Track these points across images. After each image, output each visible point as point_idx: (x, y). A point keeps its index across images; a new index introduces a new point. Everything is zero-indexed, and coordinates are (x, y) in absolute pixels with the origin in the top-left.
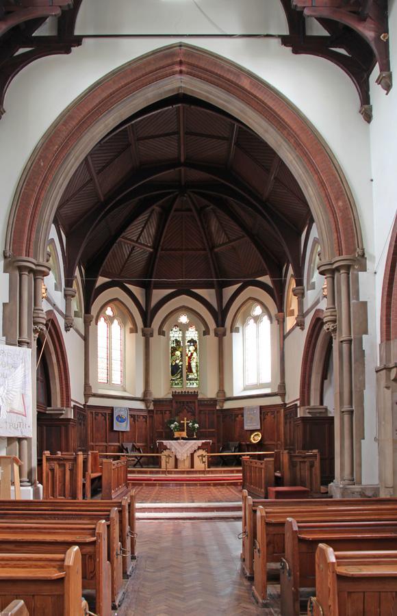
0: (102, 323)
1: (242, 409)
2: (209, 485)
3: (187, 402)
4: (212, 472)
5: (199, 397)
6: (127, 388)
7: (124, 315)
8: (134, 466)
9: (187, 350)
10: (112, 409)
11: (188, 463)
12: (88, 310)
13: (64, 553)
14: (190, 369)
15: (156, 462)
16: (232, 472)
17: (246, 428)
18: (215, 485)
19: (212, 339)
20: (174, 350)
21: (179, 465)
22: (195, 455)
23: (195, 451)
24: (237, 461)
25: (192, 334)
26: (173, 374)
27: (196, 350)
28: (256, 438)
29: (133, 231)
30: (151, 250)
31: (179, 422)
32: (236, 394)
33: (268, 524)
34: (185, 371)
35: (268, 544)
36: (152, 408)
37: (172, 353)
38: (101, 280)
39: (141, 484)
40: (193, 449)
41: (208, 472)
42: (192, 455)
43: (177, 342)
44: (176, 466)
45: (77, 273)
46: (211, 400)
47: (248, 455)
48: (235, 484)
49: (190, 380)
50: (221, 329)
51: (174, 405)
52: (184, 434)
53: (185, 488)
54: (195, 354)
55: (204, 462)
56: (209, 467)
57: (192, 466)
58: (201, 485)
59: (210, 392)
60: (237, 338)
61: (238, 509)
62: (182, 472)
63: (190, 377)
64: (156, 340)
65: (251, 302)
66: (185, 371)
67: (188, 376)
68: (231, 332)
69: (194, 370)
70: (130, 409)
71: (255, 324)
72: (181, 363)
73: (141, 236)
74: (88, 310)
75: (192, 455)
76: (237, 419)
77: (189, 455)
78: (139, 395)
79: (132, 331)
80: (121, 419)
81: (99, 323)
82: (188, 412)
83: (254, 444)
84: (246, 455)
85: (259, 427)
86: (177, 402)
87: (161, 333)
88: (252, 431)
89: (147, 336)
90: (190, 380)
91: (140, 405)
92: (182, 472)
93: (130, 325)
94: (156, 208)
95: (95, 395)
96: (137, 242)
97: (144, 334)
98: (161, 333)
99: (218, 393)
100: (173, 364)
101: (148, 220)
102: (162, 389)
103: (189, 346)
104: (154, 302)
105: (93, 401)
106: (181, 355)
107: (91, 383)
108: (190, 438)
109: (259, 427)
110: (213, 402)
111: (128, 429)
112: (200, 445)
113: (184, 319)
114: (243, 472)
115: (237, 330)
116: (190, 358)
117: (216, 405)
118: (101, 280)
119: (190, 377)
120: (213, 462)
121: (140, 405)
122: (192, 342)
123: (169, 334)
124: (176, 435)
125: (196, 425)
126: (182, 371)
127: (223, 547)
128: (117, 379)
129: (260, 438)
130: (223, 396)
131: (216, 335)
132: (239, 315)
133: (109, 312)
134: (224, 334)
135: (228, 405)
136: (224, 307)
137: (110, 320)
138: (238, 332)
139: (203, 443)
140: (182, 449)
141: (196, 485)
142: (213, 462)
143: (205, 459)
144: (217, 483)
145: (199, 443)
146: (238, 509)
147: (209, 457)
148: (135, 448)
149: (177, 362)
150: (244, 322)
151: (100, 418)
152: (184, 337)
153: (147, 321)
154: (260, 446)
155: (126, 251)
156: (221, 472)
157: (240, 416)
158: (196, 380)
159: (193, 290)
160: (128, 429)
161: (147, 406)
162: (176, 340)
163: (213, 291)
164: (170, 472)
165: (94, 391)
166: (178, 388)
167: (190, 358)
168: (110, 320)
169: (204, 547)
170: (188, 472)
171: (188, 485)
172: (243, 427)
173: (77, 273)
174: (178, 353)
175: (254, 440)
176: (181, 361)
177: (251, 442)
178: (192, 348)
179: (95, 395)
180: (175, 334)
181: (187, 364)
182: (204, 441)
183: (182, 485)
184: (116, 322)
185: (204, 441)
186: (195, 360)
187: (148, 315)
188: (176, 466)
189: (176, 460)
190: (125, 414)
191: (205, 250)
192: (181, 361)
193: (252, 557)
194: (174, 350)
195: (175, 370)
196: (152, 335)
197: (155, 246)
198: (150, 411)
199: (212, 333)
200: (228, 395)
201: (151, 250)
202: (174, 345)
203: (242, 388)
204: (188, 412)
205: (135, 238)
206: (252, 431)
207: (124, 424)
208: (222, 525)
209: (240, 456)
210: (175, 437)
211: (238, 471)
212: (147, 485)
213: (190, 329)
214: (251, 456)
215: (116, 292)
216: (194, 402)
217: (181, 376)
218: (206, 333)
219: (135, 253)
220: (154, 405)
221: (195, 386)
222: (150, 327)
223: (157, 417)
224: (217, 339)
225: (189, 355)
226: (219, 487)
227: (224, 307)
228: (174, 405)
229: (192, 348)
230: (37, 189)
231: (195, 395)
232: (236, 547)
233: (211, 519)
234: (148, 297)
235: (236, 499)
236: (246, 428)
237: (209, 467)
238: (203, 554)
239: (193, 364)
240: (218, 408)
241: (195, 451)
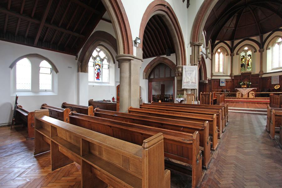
0: (217, 55)
1: (271, 77)
2: (255, 103)
3: (247, 76)
4: (257, 99)
5: (252, 74)
6: (225, 73)
7: (224, 50)
8: (227, 96)
9: (247, 58)
10: (220, 79)
11: (246, 96)
12: (212, 51)
13: (204, 123)
14: (248, 65)
15: (235, 95)
16: (265, 99)
17: (272, 83)
18: (257, 103)
19: (258, 54)
21: (243, 96)
22: (250, 93)
23: (250, 92)
24: (268, 95)
25: (249, 53)
26: (241, 67)
27: (251, 58)
28: (277, 87)
29: (227, 24)
30: (234, 28)
31: (243, 82)
32: (267, 72)
33: (276, 115)
35: (276, 122)
36: (233, 78)
37: (241, 60)
38: (217, 42)
39: (229, 102)
40: (249, 91)
41: (255, 99)
42: (248, 93)
43: (243, 56)
44: (242, 97)
45: (209, 42)
46: (257, 74)
47: (272, 93)
48: (267, 104)
49: (248, 68)
50: (262, 49)
51: (242, 77)
52: (245, 86)
53: (245, 103)
54: (250, 60)
55: (253, 96)
56: (255, 97)
57: (248, 97)
58: (252, 103)
59: (257, 71)
60: (269, 52)
61: (266, 111)
62: (245, 99)
63: (248, 67)
64: (236, 57)
65: (276, 37)
68: (267, 50)
69: (250, 65)
70: (226, 79)
71: (278, 45)
73: (231, 24)
74: (212, 51)
75: (248, 93)
76: (269, 80)
77: (247, 93)
78: (229, 74)
79: (227, 55)
80: (222, 82)
81: (216, 54)
82: (247, 79)
83: (276, 89)
84: (271, 93)
85: (279, 83)
86: (242, 76)
87: (237, 54)
88: (275, 85)
89: (232, 56)
90: (248, 68)
91: (229, 78)
92: (245, 99)
93: (226, 54)
94: (236, 14)
95: (214, 76)
96: (229, 27)
97: (231, 55)
98: (237, 54)
99: (260, 72)
101: (233, 19)
102: (237, 72)
103: (248, 57)
104: (235, 44)
105: (213, 78)
107: (213, 72)
108: (248, 87)
109: (279, 83)
110: (258, 75)
111: (225, 85)
112: (252, 90)
113: (246, 48)
114: (270, 99)
115: (269, 49)
116: (248, 61)
117: (259, 76)
118: (217, 42)
119: (248, 67)
120: (257, 96)
121: (229, 78)
122: (250, 55)
123: (240, 54)
124: (242, 86)
125: (250, 83)
126: (245, 66)
127: (259, 122)
128: (221, 70)
129: (279, 87)
130: (262, 72)
131: (260, 51)
132: (270, 43)
133: (219, 50)
134: (263, 51)
135: (264, 76)
136: (263, 41)
137: (219, 53)
138: (270, 49)
139: (253, 89)
140: (245, 91)
141: (250, 103)
142: (257, 96)
143: (254, 95)
144: (258, 103)
145: (252, 89)
146: (266, 111)
147: (255, 94)
148: (227, 91)
149: (243, 63)
150: (273, 45)
151: (216, 82)
152: (246, 55)
153: (232, 51)
154: (279, 90)
155: (225, 31)
156: (260, 99)
157: (270, 79)
158: (251, 68)
159: (251, 38)
160: (225, 85)
161: (231, 78)
162: (243, 56)
163: (259, 37)
164: (240, 99)
165: (214, 75)
166: (243, 72)
167: (248, 61)
168: (219, 53)
169: (251, 121)
170: (247, 99)
171: (246, 103)
172: (271, 82)
173: (209, 42)
174: (244, 60)
175: (276, 88)
177: (275, 88)
178: (249, 58)
179: (214, 76)
180: (243, 54)
181: (247, 63)
182: (253, 88)
183: (244, 103)
184: (221, 53)
185: (253, 88)
186: (250, 62)
187: (232, 50)
188: (242, 97)
189: (242, 95)
190: (224, 81)
191: (255, 23)
193: (270, 125)
194: (242, 59)
195: (242, 65)
196: (234, 55)
197: (235, 27)
198: (233, 79)
199: (258, 51)
200: (264, 72)
201: (234, 28)
202: (242, 57)
203: (271, 69)
204: (247, 79)
205: (228, 26)
206: (275, 85)
207: (223, 84)
208: (259, 116)
209: (269, 94)
210: (242, 87)
211: (268, 99)
212: (231, 102)
213: (249, 51)
214: (274, 93)
215: (222, 44)
216: (250, 76)
217: (245, 67)
218: (255, 51)
219: (228, 31)
220: (234, 77)
221: (250, 70)
222: (233, 53)
223: (235, 81)
224: (260, 53)
225: (248, 60)
226: (259, 104)
227: (263, 41)
228: (242, 77)
229: (249, 58)
230: (199, 23)
231: (250, 73)
232: (265, 123)
233: (255, 114)
234: (232, 43)
235: (264, 108)
236: (272, 83)
237: (255, 97)
238: (251, 124)
239: (250, 63)
240: (260, 77)
241: (250, 92)
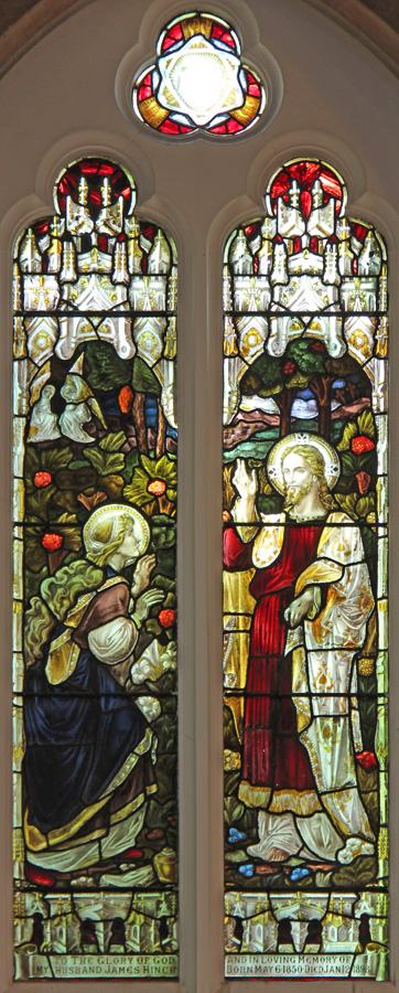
9: (245, 483)
14: (270, 741)
20: (64, 485)
26: (52, 794)
34: (204, 760)
37: (40, 522)
43: (113, 383)
49: (277, 877)
54: (340, 542)
63: (275, 838)
66: (204, 760)
67: (244, 827)
69: (328, 758)
72: (155, 659)
90: (277, 877)
100: (56, 675)
106: (163, 552)
116: (273, 589)
119: (275, 838)
122: (308, 377)
126: (164, 768)
149: (113, 637)
152: (197, 314)
158: (356, 878)
162: (96, 351)
167: (273, 589)
174: (118, 526)
176: (160, 626)
181: (237, 675)
186: (339, 628)
192: (160, 626)
194: (64, 485)
217: (162, 833)
225: (266, 551)
239: (321, 671)
